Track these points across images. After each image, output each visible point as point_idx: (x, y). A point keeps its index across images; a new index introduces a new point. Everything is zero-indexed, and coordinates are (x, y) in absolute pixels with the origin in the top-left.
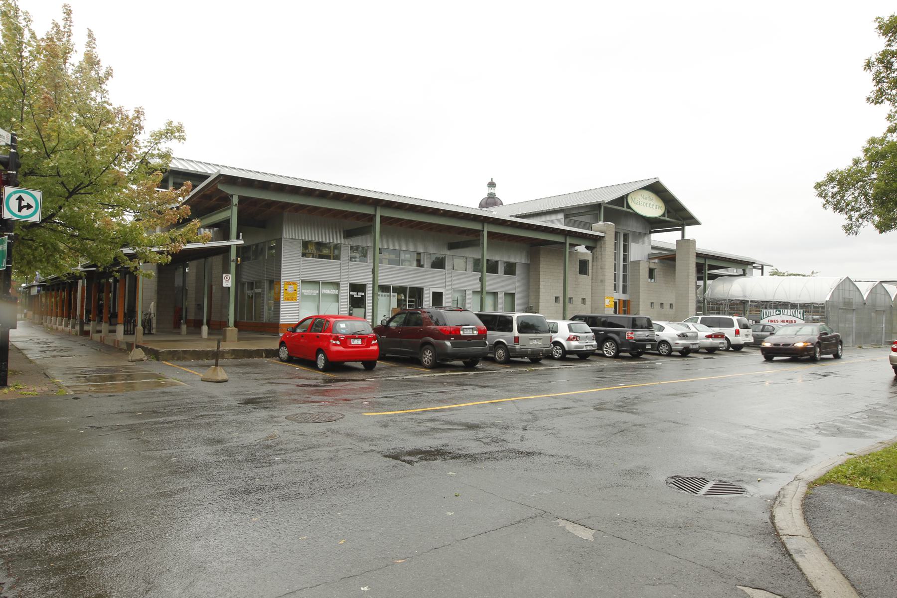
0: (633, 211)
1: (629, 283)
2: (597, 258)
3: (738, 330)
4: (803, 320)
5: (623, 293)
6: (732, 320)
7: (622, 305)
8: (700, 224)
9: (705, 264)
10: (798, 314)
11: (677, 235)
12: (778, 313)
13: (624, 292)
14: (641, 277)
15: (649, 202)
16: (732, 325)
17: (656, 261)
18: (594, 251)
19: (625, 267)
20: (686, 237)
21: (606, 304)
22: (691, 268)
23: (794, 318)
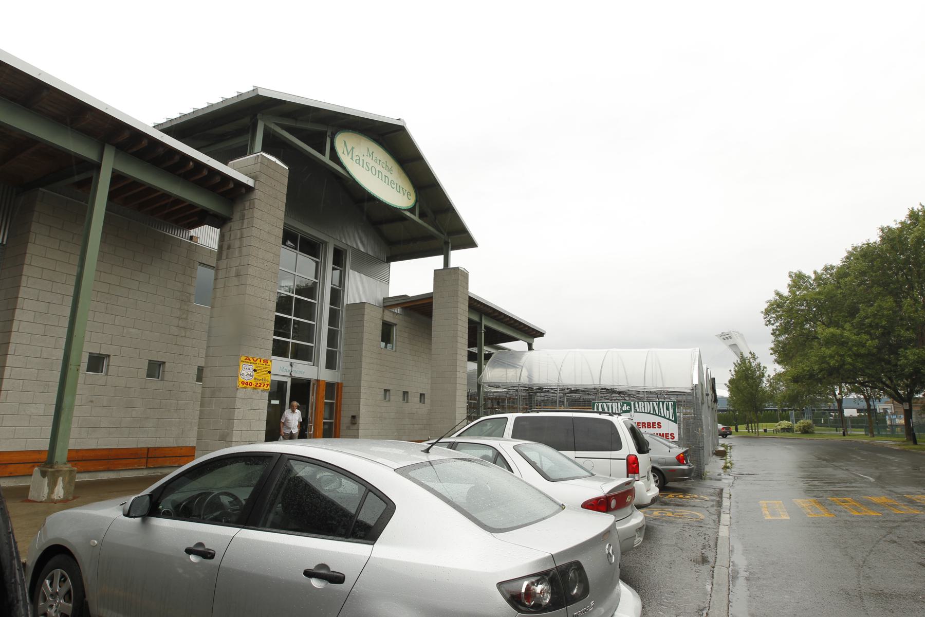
0: (348, 172)
1: (341, 349)
2: (229, 248)
3: (636, 459)
4: (675, 422)
5: (327, 367)
6: (611, 425)
7: (323, 393)
8: (477, 247)
9: (480, 324)
10: (664, 411)
11: (437, 262)
12: (625, 408)
13: (331, 364)
14: (366, 335)
15: (385, 172)
16: (612, 442)
17: (398, 310)
18: (227, 227)
19: (334, 317)
20: (453, 264)
21: (241, 379)
22: (460, 323)
23: (656, 419)
